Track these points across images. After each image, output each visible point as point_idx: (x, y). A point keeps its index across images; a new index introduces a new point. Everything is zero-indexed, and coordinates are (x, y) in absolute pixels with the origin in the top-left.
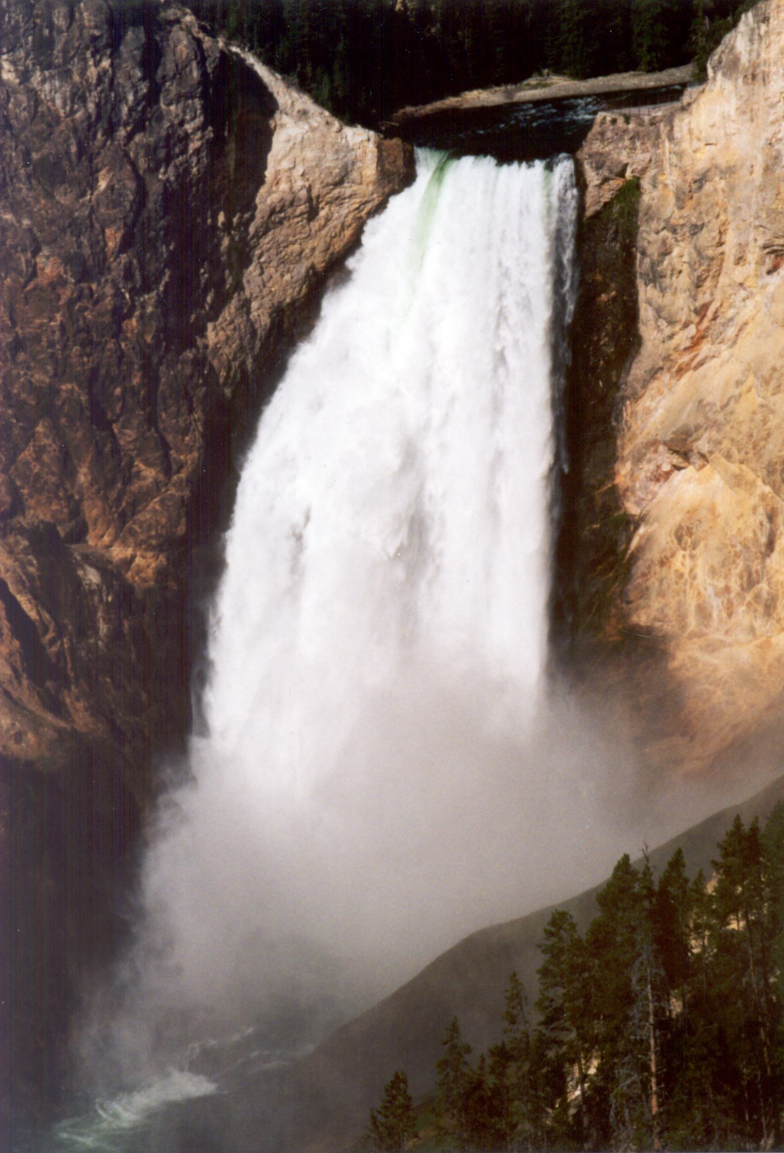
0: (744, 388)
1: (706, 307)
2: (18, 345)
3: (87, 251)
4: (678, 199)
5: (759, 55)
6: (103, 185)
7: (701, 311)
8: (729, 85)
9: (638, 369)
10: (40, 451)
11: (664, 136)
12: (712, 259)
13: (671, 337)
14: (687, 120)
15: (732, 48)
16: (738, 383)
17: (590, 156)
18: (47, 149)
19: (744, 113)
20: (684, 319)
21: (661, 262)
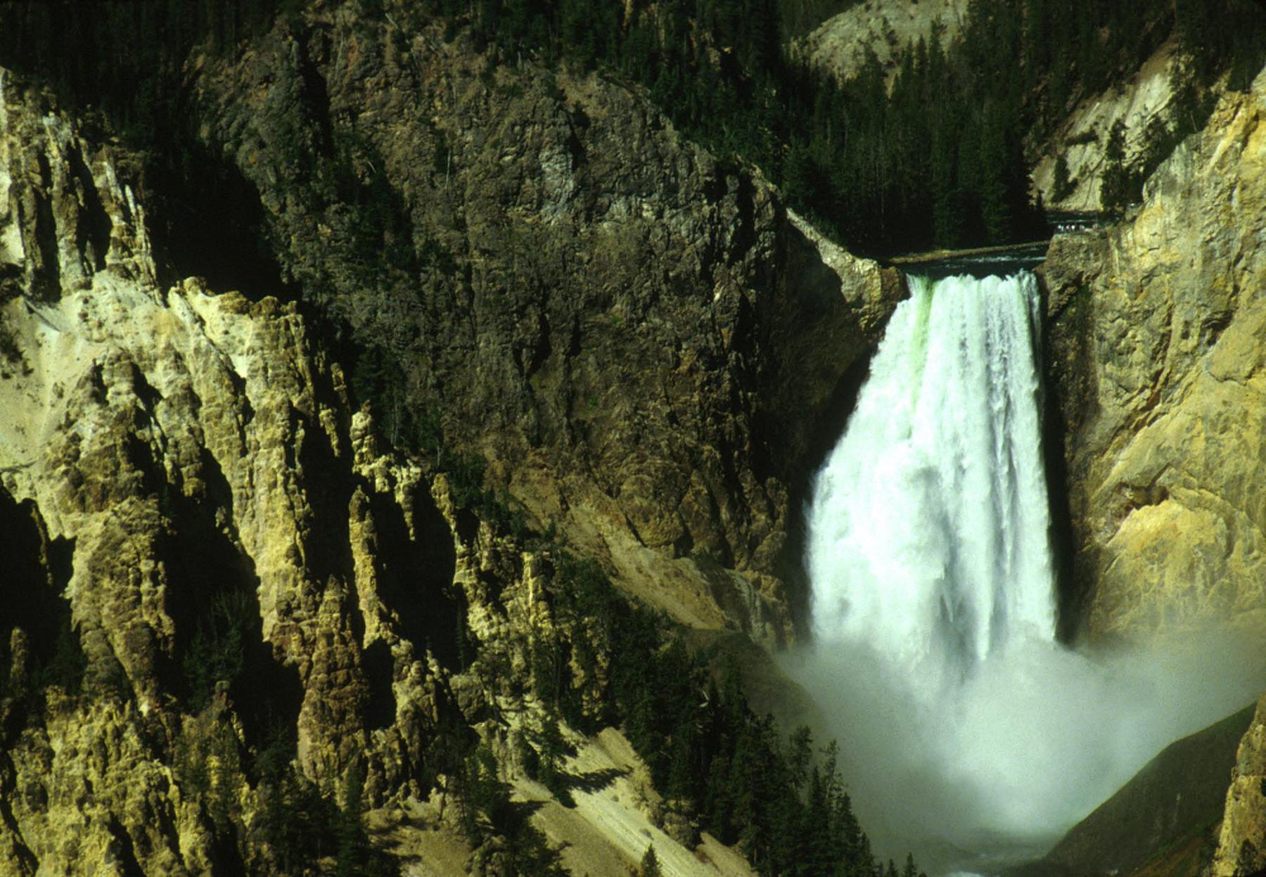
0: (1195, 432)
1: (1159, 373)
2: (672, 418)
3: (712, 345)
4: (1129, 292)
5: (1193, 176)
6: (717, 296)
7: (1155, 378)
8: (1168, 201)
9: (1098, 431)
10: (698, 493)
11: (1113, 247)
12: (1163, 335)
13: (1129, 401)
14: (1130, 234)
15: (1167, 174)
16: (1188, 430)
17: (1052, 268)
18: (680, 267)
19: (1183, 220)
20: (1140, 386)
21: (1118, 344)
